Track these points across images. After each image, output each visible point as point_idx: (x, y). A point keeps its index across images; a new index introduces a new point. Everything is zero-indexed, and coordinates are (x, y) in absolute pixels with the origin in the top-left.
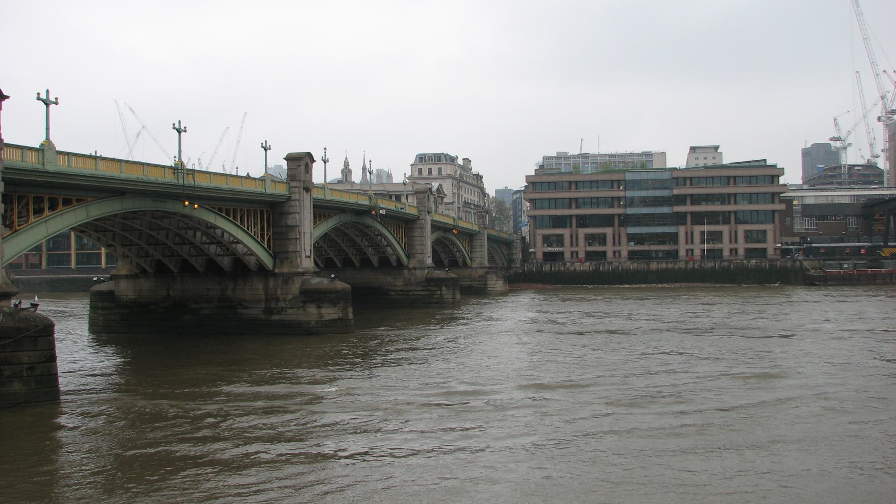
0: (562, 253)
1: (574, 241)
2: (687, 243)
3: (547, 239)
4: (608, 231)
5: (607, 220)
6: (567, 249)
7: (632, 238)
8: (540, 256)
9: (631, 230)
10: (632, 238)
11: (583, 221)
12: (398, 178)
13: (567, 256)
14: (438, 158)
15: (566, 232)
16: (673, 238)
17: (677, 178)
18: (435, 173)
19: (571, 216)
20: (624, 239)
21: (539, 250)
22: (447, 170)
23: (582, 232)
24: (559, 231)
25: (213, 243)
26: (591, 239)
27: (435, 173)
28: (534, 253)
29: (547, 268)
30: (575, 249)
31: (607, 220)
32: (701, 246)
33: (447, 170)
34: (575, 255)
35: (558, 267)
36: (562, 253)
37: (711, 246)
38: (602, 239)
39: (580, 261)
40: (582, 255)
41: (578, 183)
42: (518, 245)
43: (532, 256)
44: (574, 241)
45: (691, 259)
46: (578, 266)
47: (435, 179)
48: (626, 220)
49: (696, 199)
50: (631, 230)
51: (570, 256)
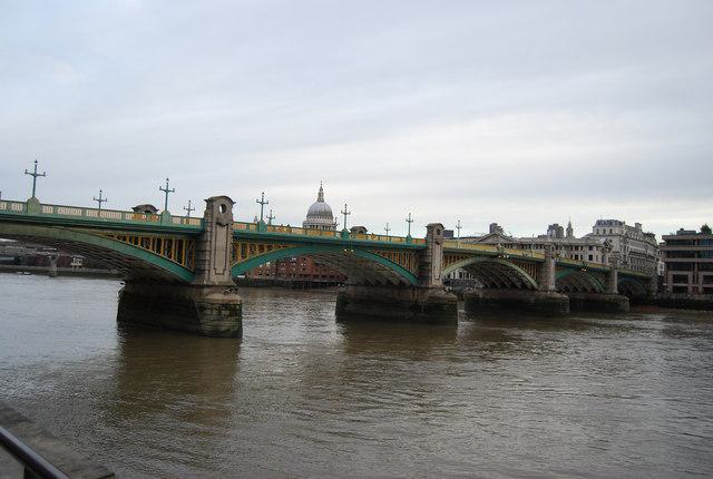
0: (687, 288)
1: (695, 279)
3: (676, 279)
6: (690, 285)
8: (670, 289)
12: (579, 234)
13: (690, 289)
14: (610, 223)
15: (690, 274)
18: (608, 232)
21: (670, 285)
22: (616, 230)
23: (702, 274)
24: (685, 273)
27: (608, 232)
29: (673, 297)
33: (616, 230)
35: (681, 296)
36: (687, 288)
44: (695, 279)
46: (697, 297)
47: (603, 236)
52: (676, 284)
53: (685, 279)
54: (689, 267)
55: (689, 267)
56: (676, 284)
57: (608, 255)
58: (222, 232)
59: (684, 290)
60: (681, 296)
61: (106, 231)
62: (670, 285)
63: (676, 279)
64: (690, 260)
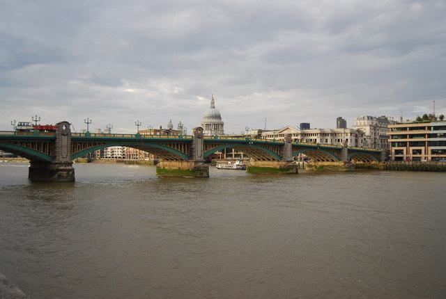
4: (423, 148)
5: (422, 144)
6: (405, 155)
7: (433, 152)
8: (393, 158)
13: (405, 158)
20: (430, 152)
21: (393, 156)
24: (402, 148)
26: (415, 152)
31: (422, 144)
38: (420, 151)
42: (384, 153)
46: (407, 163)
48: (431, 144)
49: (411, 136)
52: (397, 156)
54: (404, 144)
55: (404, 144)
56: (397, 156)
57: (360, 139)
58: (200, 141)
59: (401, 159)
60: (399, 163)
62: (393, 156)
64: (404, 140)
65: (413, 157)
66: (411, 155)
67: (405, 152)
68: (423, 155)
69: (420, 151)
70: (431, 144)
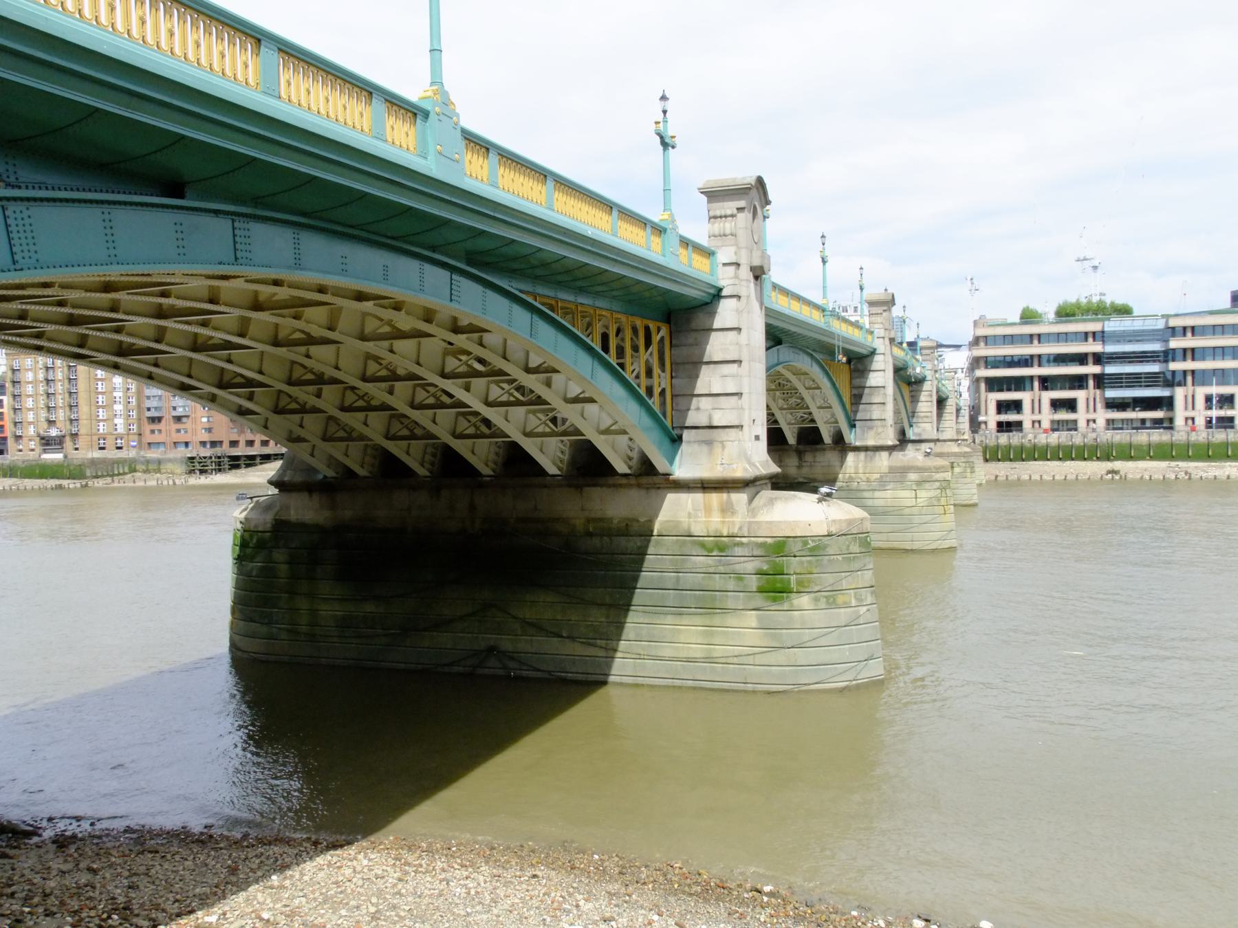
1: (1036, 406)
2: (1186, 408)
4: (1080, 395)
5: (1078, 382)
7: (1112, 405)
8: (992, 425)
9: (1111, 393)
10: (1112, 405)
11: (1046, 383)
13: (1027, 425)
16: (1168, 403)
17: (1173, 328)
19: (1031, 378)
25: (518, 403)
26: (1056, 405)
28: (986, 423)
30: (1036, 417)
31: (1078, 382)
32: (1209, 413)
34: (1037, 425)
37: (1222, 413)
38: (1071, 405)
39: (1046, 431)
40: (1046, 424)
41: (1042, 337)
43: (983, 426)
44: (1036, 406)
45: (1193, 429)
46: (1042, 439)
48: (1100, 380)
50: (1111, 393)
51: (1031, 426)
53: (1017, 406)
54: (1018, 383)
60: (1015, 438)
61: (540, 290)
63: (1002, 407)
65: (1053, 422)
66: (1047, 416)
67: (1026, 406)
68: (1081, 416)
69: (1071, 405)
70: (1100, 380)
